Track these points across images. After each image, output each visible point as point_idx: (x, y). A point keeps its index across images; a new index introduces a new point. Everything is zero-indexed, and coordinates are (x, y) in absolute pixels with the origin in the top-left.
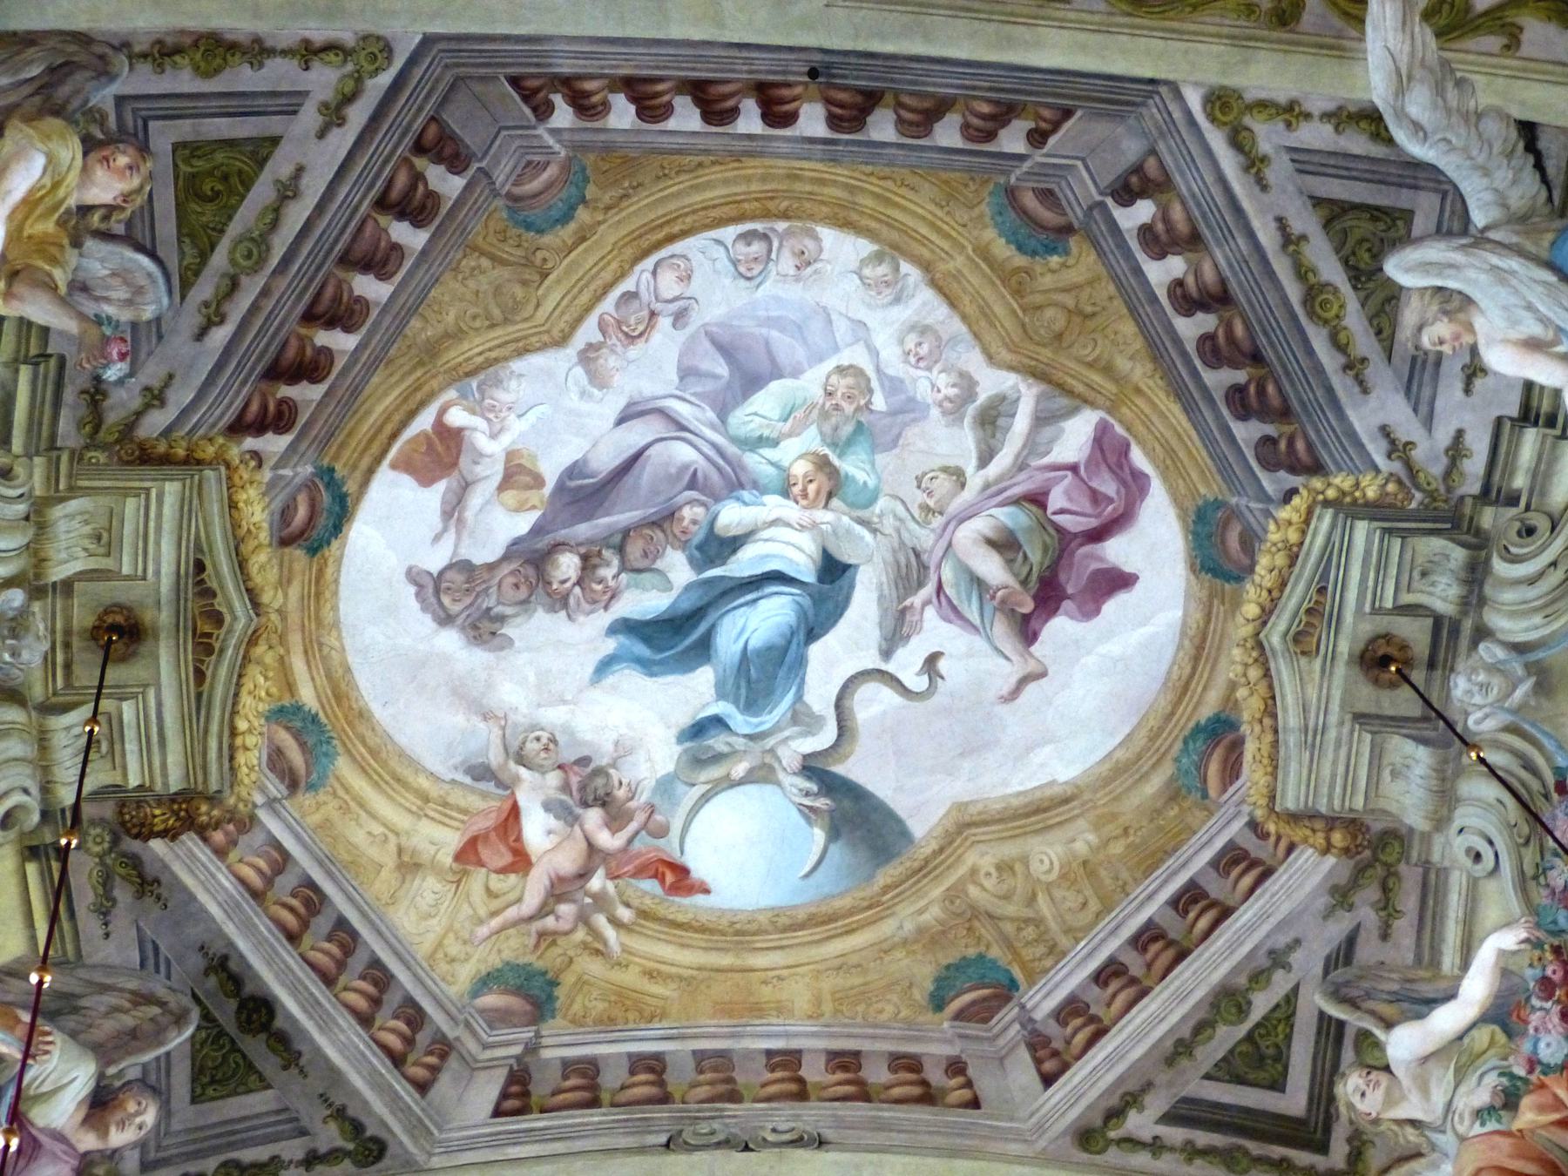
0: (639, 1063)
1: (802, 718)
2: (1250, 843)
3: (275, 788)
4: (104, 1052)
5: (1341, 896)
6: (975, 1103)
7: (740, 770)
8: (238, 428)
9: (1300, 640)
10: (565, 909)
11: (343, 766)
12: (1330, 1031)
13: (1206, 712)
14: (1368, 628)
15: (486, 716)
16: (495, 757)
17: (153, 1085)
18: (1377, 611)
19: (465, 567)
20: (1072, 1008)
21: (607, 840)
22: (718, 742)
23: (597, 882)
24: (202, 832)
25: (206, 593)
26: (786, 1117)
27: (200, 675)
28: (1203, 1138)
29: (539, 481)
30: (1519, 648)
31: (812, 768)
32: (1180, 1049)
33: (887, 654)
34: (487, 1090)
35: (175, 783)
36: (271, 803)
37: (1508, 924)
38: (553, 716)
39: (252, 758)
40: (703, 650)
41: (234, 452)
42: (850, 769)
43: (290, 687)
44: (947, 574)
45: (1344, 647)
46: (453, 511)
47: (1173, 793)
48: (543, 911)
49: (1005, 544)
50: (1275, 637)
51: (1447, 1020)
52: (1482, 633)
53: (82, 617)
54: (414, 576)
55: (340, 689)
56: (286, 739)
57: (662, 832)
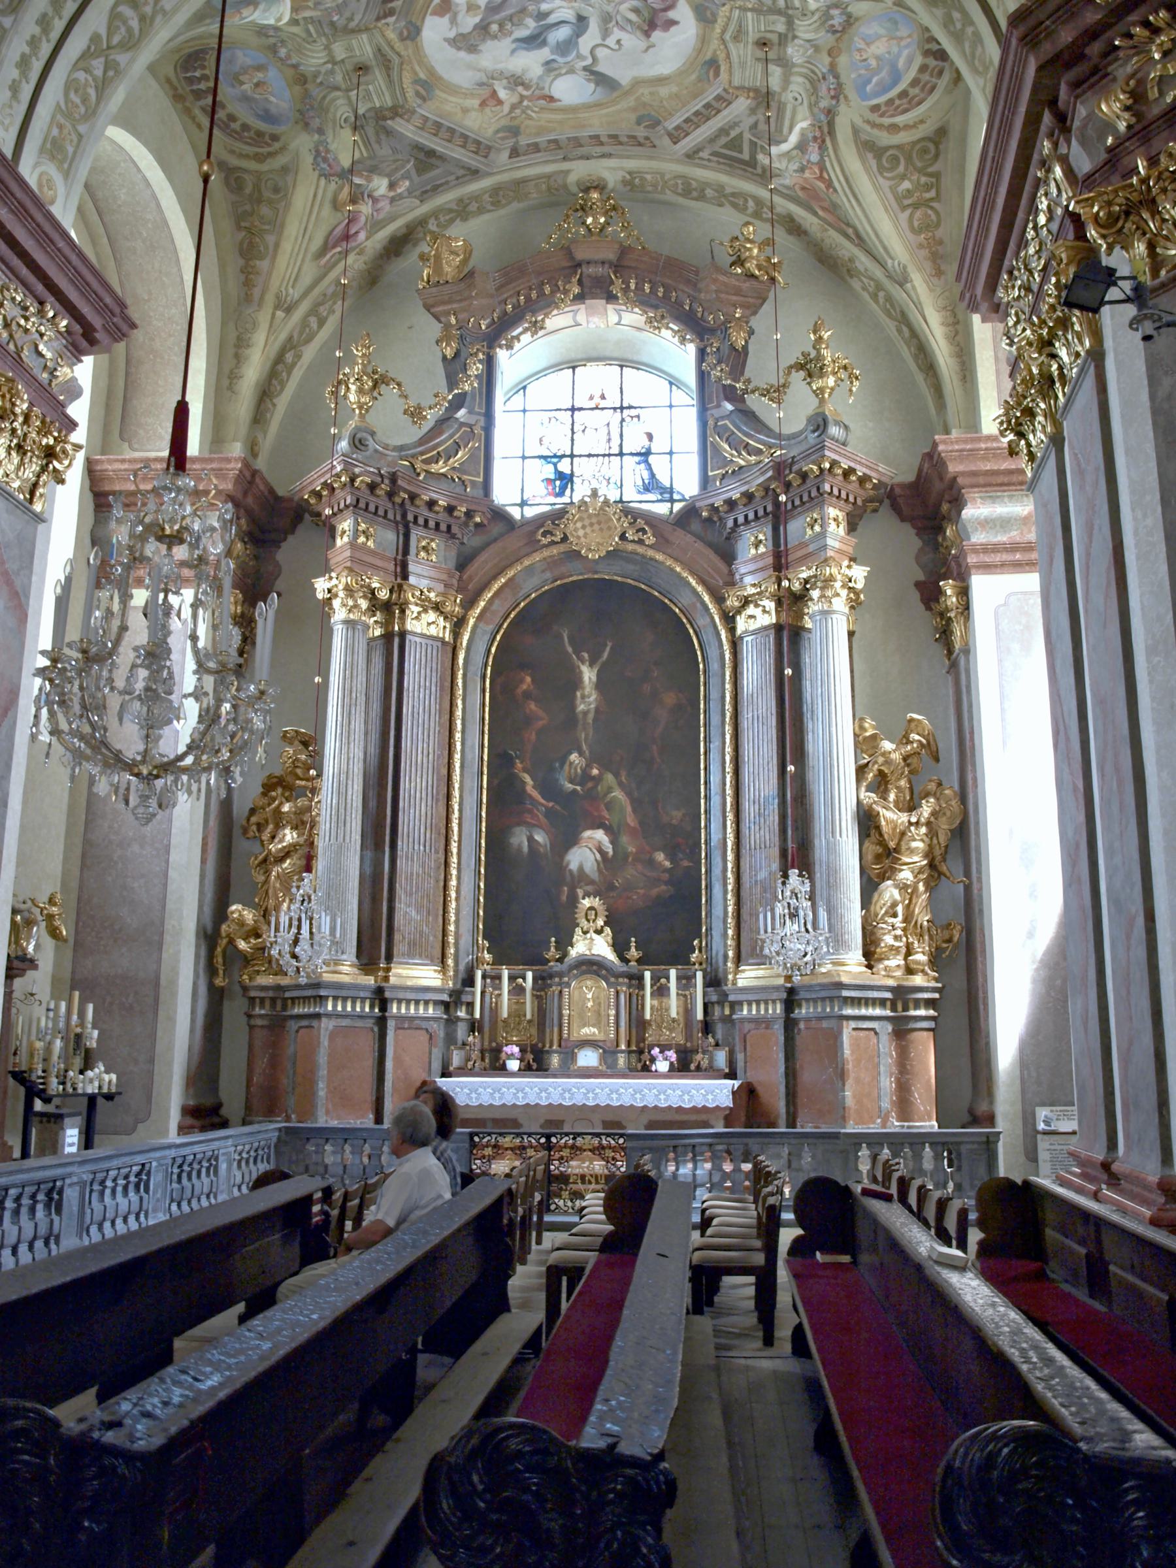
0: (549, 141)
1: (580, 57)
2: (724, 94)
3: (419, 101)
4: (388, 175)
5: (753, 111)
6: (654, 146)
7: (564, 71)
8: (378, 19)
9: (736, 38)
10: (518, 111)
11: (437, 92)
12: (753, 145)
13: (708, 56)
14: (757, 36)
15: (479, 70)
16: (485, 80)
17: (406, 176)
18: (759, 31)
19: (462, 35)
20: (677, 128)
21: (525, 93)
22: (555, 65)
23: (525, 103)
24: (401, 116)
25: (383, 55)
26: (599, 150)
27: (389, 76)
28: (721, 160)
29: (479, 7)
30: (808, 41)
31: (585, 69)
32: (712, 140)
33: (604, 40)
34: (506, 154)
35: (390, 104)
36: (419, 106)
37: (805, 119)
38: (501, 66)
39: (410, 94)
40: (544, 43)
41: (379, 25)
42: (600, 68)
43: (416, 74)
44: (619, 18)
45: (750, 40)
46: (453, 21)
47: (699, 80)
48: (511, 112)
49: (636, 10)
50: (727, 37)
51: (785, 147)
52: (795, 37)
53: (349, 67)
54: (446, 40)
55: (432, 72)
56: (419, 88)
57: (543, 88)
